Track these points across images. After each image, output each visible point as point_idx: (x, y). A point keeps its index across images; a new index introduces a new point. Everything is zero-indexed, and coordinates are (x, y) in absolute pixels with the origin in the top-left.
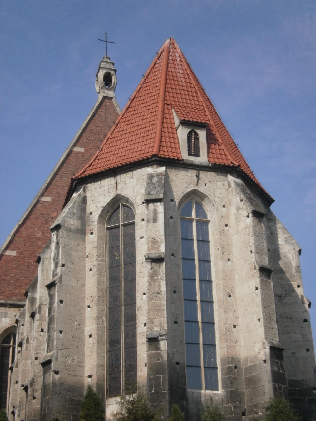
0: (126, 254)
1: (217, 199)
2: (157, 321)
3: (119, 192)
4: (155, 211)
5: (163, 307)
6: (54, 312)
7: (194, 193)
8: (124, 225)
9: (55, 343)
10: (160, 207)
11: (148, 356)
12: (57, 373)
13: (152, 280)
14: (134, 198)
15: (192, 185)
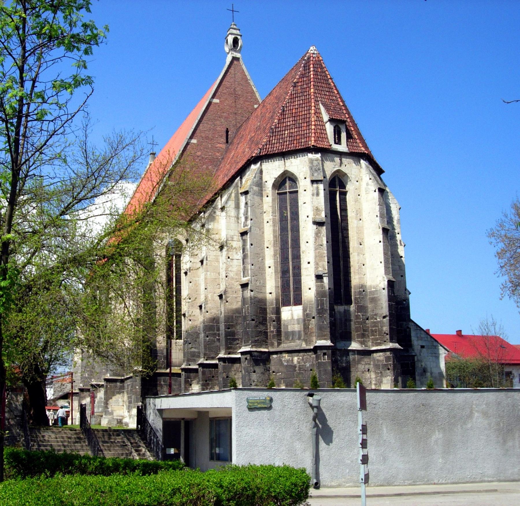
0: (292, 213)
1: (353, 176)
2: (320, 264)
3: (287, 169)
4: (318, 188)
5: (324, 255)
6: (247, 251)
7: (338, 171)
8: (290, 192)
9: (250, 272)
10: (321, 186)
11: (317, 286)
12: (252, 291)
13: (317, 236)
14: (298, 174)
15: (337, 166)
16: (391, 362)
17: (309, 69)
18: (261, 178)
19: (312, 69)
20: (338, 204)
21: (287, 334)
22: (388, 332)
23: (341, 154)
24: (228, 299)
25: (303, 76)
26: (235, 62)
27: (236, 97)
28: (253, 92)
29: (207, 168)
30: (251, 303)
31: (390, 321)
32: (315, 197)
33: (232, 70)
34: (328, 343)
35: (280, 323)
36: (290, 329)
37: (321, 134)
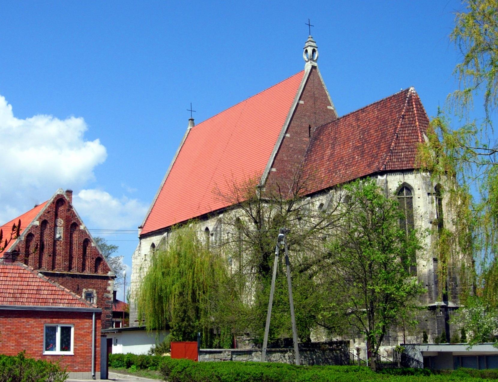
3: (405, 181)
17: (412, 105)
19: (414, 106)
25: (408, 111)
26: (314, 70)
27: (315, 99)
28: (326, 95)
29: (297, 157)
33: (311, 77)
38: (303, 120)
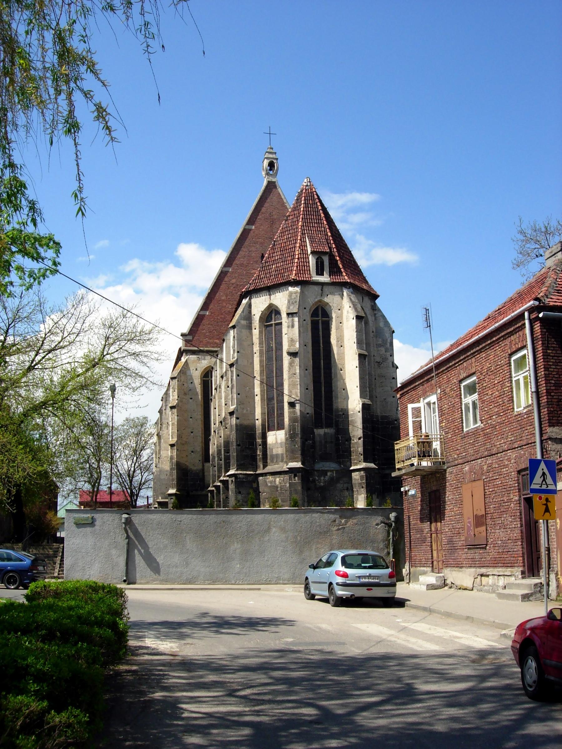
1: (335, 305)
2: (294, 391)
3: (272, 302)
4: (293, 322)
7: (320, 301)
16: (364, 481)
18: (250, 312)
19: (303, 202)
20: (321, 333)
21: (272, 457)
22: (362, 452)
23: (322, 284)
24: (227, 426)
30: (237, 430)
31: (364, 441)
32: (290, 329)
34: (298, 465)
35: (266, 446)
36: (274, 452)
37: (303, 267)
38: (253, 249)
